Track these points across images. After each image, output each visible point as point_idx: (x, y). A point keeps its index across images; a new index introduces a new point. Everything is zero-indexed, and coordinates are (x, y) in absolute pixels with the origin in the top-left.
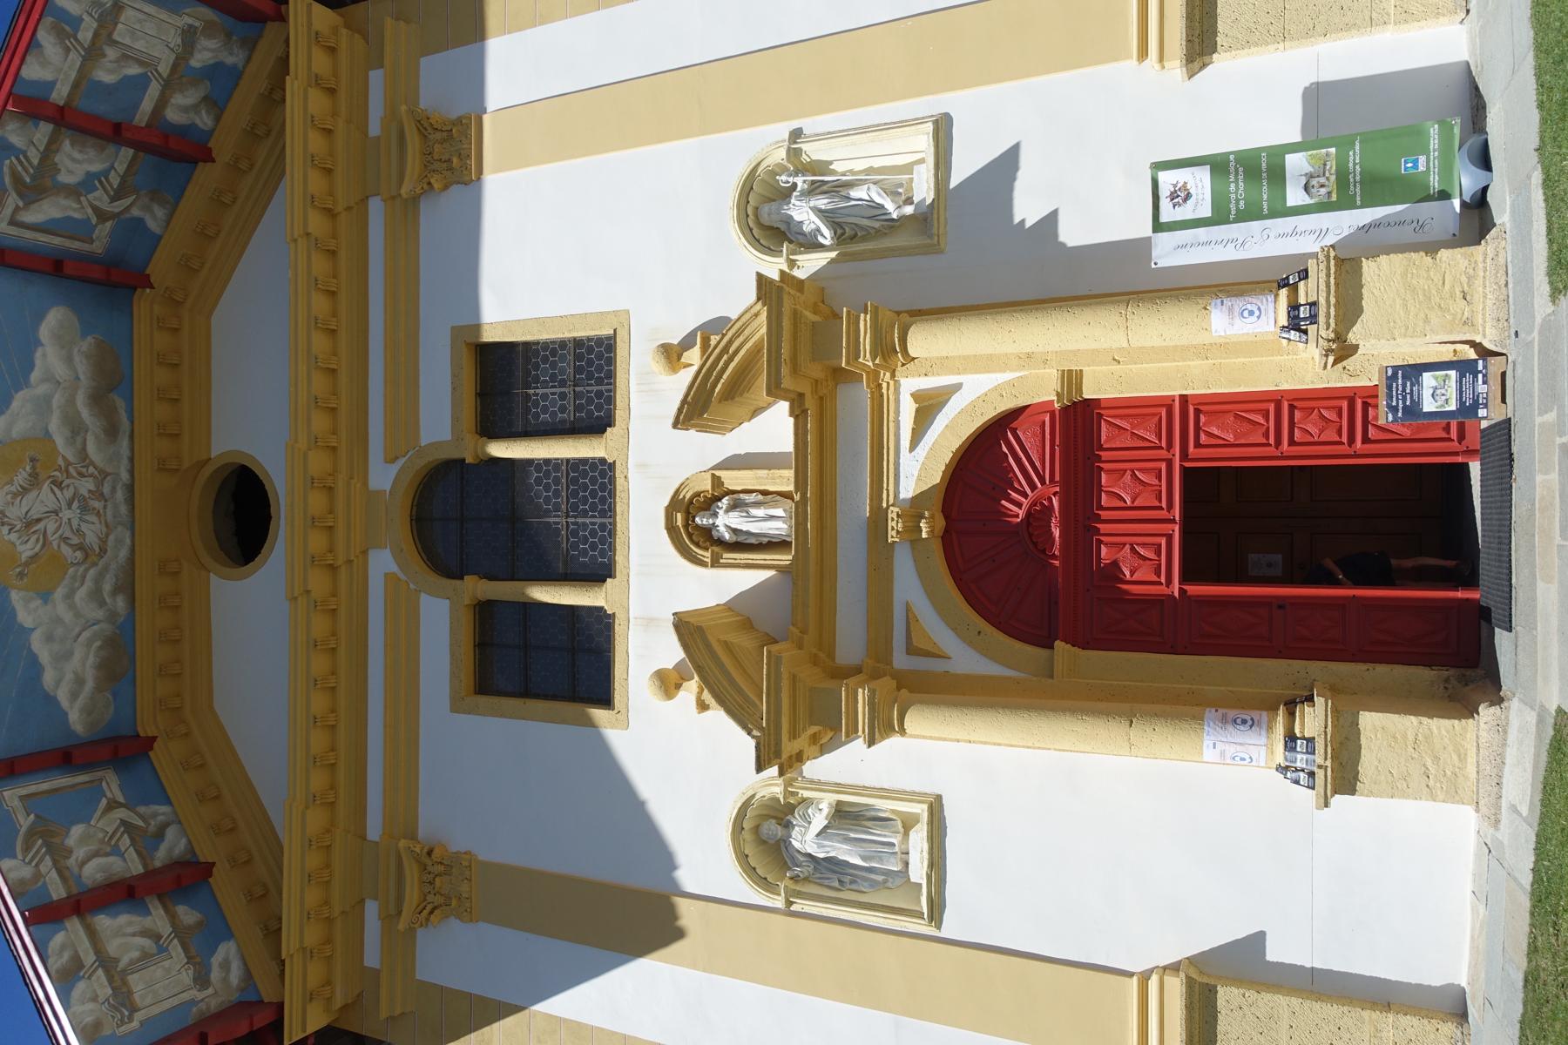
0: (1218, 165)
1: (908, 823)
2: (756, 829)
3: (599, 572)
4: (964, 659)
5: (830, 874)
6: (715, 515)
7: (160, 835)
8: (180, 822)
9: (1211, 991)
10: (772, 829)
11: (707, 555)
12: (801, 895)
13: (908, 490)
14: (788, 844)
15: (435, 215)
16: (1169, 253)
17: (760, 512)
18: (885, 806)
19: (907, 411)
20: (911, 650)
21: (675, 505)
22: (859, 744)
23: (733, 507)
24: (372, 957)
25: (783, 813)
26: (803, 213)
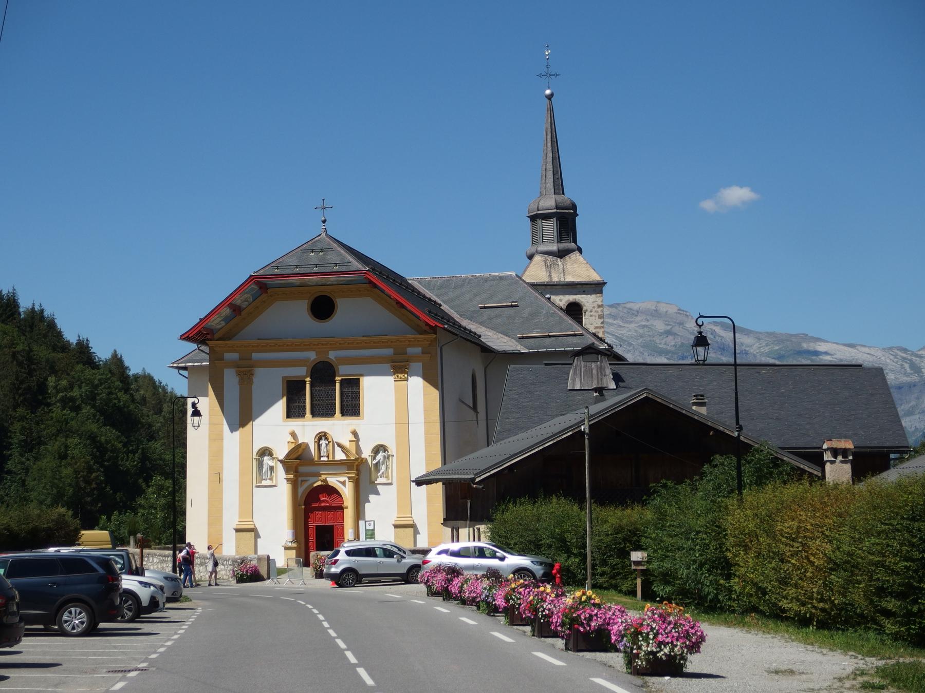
0: (373, 530)
1: (271, 479)
2: (267, 450)
3: (314, 414)
4: (301, 490)
5: (260, 465)
6: (324, 440)
7: (247, 301)
8: (250, 304)
9: (253, 531)
10: (267, 453)
11: (316, 440)
12: (256, 460)
13: (328, 479)
14: (265, 456)
15: (387, 366)
16: (361, 523)
17: (325, 450)
18: (274, 475)
19: (342, 479)
20: (302, 481)
21: (325, 433)
22: (285, 476)
23: (327, 445)
24: (228, 356)
25: (270, 454)
26: (380, 456)
